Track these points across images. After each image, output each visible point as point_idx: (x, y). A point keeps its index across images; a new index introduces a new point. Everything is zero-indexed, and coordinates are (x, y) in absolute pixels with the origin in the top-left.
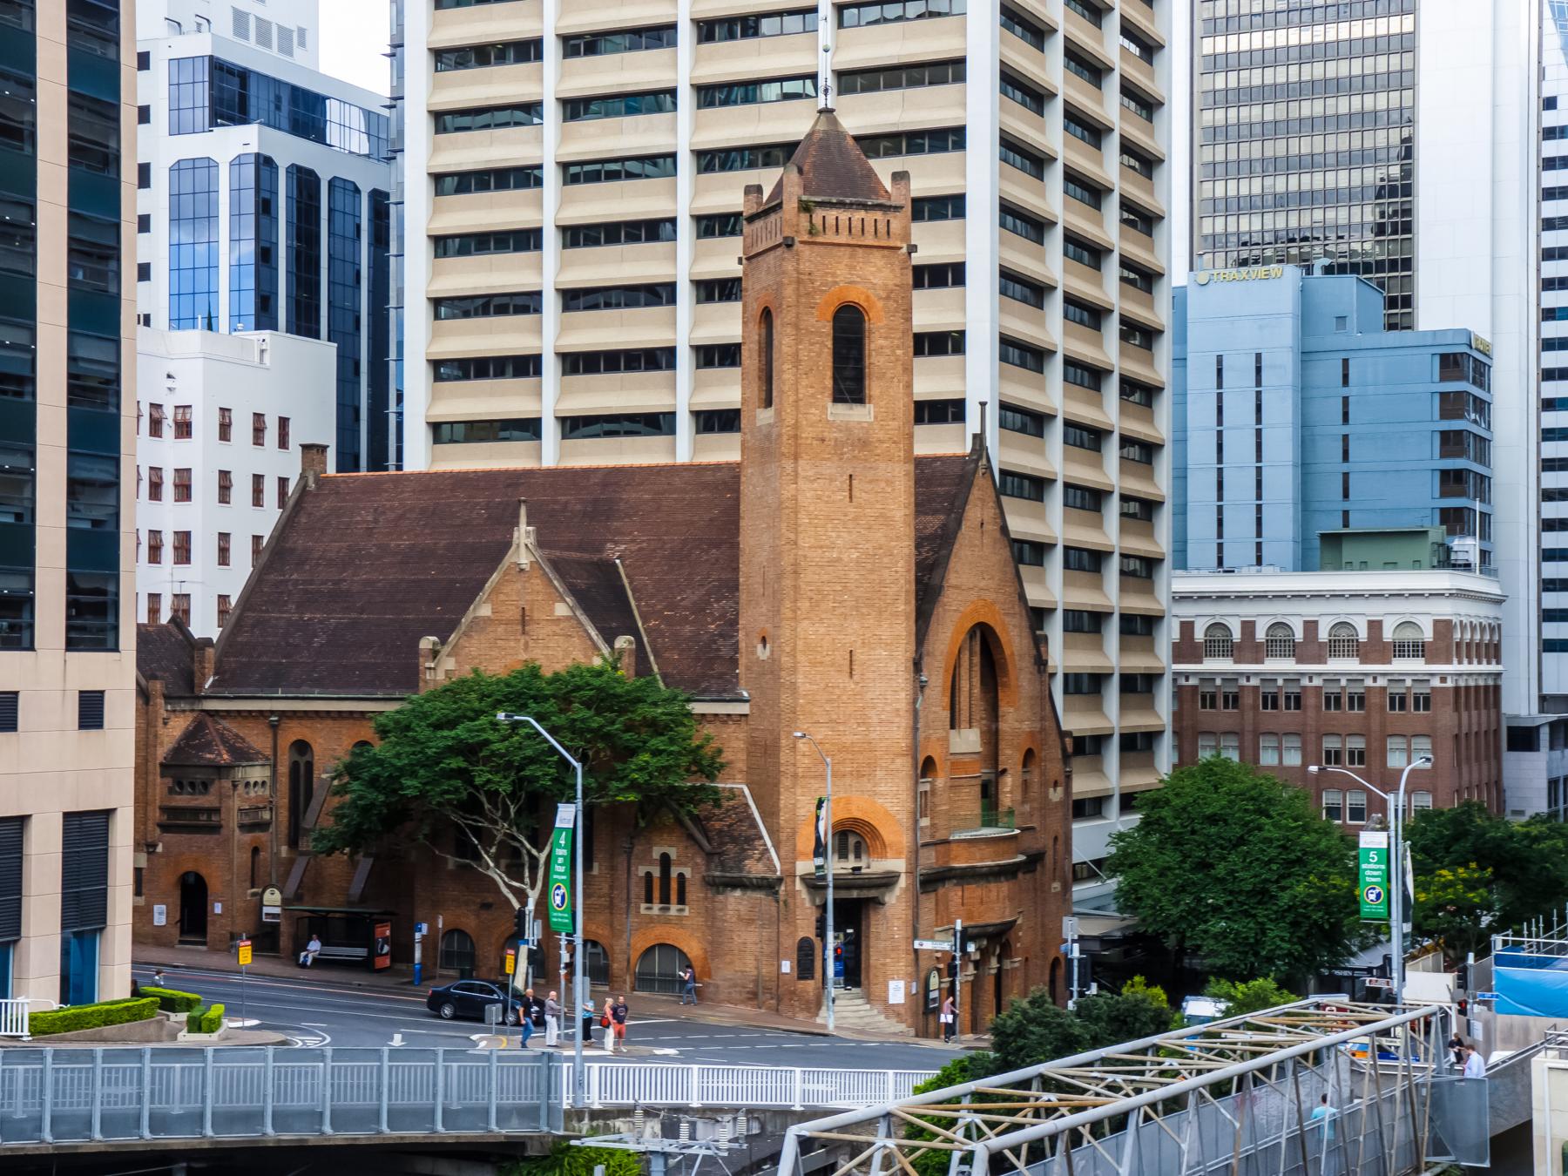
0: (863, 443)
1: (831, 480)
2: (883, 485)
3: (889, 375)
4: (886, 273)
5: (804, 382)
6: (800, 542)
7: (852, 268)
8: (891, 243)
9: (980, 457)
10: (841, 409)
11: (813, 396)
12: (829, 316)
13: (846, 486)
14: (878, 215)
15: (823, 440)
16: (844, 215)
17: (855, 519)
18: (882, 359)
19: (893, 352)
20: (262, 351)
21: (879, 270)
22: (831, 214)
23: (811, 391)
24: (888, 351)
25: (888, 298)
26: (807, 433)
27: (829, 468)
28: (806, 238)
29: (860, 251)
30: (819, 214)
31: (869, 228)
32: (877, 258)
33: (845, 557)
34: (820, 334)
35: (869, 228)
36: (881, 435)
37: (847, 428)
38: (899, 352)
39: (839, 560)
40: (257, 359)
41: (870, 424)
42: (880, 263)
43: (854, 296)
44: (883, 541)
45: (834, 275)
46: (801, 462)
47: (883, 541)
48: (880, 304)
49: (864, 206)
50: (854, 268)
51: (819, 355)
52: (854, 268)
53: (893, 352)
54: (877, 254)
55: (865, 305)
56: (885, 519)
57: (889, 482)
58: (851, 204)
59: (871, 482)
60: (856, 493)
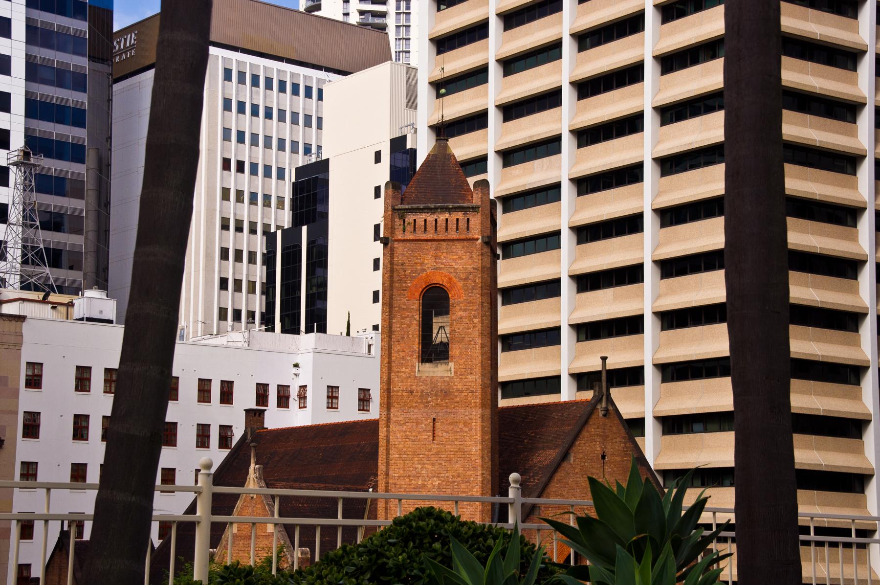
0: (445, 393)
1: (418, 423)
2: (461, 426)
3: (467, 339)
4: (466, 259)
5: (396, 347)
6: (391, 473)
7: (436, 257)
8: (470, 236)
9: (600, 400)
10: (427, 368)
11: (403, 358)
12: (417, 295)
13: (430, 428)
14: (460, 215)
15: (411, 392)
16: (431, 218)
17: (437, 453)
18: (461, 327)
19: (471, 321)
20: (370, 346)
21: (460, 258)
22: (421, 218)
23: (402, 354)
24: (467, 321)
25: (466, 279)
26: (398, 386)
27: (415, 414)
28: (400, 236)
29: (444, 244)
30: (410, 218)
31: (452, 225)
32: (458, 248)
33: (429, 485)
34: (407, 310)
35: (452, 225)
36: (460, 387)
37: (432, 381)
38: (475, 321)
39: (424, 486)
40: (364, 350)
41: (452, 378)
42: (461, 252)
43: (438, 279)
44: (461, 470)
45: (422, 264)
46: (392, 410)
47: (461, 470)
48: (460, 284)
49: (450, 210)
50: (439, 258)
51: (409, 326)
52: (439, 258)
53: (471, 321)
54: (459, 245)
55: (448, 285)
56: (462, 453)
57: (466, 424)
58: (436, 208)
59: (451, 424)
60: (438, 433)
